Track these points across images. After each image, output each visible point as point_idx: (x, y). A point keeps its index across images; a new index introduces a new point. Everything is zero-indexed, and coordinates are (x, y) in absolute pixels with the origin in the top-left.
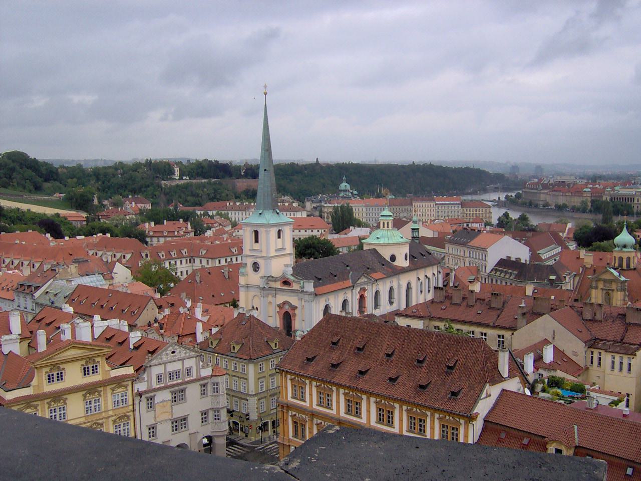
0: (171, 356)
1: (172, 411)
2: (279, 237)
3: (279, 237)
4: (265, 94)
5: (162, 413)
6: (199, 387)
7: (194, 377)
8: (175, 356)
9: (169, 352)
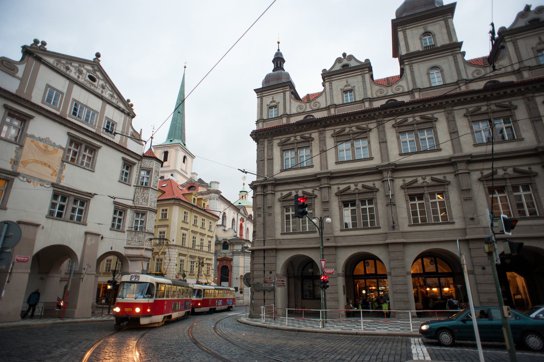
0: (84, 79)
1: (61, 171)
2: (184, 162)
3: (184, 162)
4: (185, 67)
5: (37, 162)
6: (120, 163)
7: (117, 139)
8: (93, 84)
9: (85, 71)
